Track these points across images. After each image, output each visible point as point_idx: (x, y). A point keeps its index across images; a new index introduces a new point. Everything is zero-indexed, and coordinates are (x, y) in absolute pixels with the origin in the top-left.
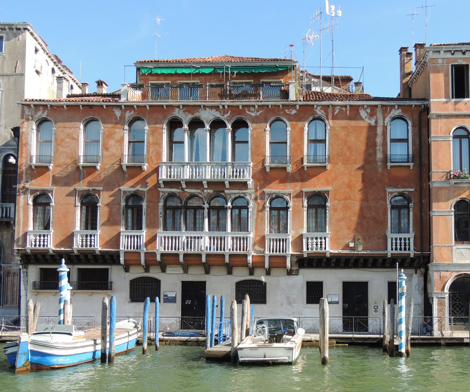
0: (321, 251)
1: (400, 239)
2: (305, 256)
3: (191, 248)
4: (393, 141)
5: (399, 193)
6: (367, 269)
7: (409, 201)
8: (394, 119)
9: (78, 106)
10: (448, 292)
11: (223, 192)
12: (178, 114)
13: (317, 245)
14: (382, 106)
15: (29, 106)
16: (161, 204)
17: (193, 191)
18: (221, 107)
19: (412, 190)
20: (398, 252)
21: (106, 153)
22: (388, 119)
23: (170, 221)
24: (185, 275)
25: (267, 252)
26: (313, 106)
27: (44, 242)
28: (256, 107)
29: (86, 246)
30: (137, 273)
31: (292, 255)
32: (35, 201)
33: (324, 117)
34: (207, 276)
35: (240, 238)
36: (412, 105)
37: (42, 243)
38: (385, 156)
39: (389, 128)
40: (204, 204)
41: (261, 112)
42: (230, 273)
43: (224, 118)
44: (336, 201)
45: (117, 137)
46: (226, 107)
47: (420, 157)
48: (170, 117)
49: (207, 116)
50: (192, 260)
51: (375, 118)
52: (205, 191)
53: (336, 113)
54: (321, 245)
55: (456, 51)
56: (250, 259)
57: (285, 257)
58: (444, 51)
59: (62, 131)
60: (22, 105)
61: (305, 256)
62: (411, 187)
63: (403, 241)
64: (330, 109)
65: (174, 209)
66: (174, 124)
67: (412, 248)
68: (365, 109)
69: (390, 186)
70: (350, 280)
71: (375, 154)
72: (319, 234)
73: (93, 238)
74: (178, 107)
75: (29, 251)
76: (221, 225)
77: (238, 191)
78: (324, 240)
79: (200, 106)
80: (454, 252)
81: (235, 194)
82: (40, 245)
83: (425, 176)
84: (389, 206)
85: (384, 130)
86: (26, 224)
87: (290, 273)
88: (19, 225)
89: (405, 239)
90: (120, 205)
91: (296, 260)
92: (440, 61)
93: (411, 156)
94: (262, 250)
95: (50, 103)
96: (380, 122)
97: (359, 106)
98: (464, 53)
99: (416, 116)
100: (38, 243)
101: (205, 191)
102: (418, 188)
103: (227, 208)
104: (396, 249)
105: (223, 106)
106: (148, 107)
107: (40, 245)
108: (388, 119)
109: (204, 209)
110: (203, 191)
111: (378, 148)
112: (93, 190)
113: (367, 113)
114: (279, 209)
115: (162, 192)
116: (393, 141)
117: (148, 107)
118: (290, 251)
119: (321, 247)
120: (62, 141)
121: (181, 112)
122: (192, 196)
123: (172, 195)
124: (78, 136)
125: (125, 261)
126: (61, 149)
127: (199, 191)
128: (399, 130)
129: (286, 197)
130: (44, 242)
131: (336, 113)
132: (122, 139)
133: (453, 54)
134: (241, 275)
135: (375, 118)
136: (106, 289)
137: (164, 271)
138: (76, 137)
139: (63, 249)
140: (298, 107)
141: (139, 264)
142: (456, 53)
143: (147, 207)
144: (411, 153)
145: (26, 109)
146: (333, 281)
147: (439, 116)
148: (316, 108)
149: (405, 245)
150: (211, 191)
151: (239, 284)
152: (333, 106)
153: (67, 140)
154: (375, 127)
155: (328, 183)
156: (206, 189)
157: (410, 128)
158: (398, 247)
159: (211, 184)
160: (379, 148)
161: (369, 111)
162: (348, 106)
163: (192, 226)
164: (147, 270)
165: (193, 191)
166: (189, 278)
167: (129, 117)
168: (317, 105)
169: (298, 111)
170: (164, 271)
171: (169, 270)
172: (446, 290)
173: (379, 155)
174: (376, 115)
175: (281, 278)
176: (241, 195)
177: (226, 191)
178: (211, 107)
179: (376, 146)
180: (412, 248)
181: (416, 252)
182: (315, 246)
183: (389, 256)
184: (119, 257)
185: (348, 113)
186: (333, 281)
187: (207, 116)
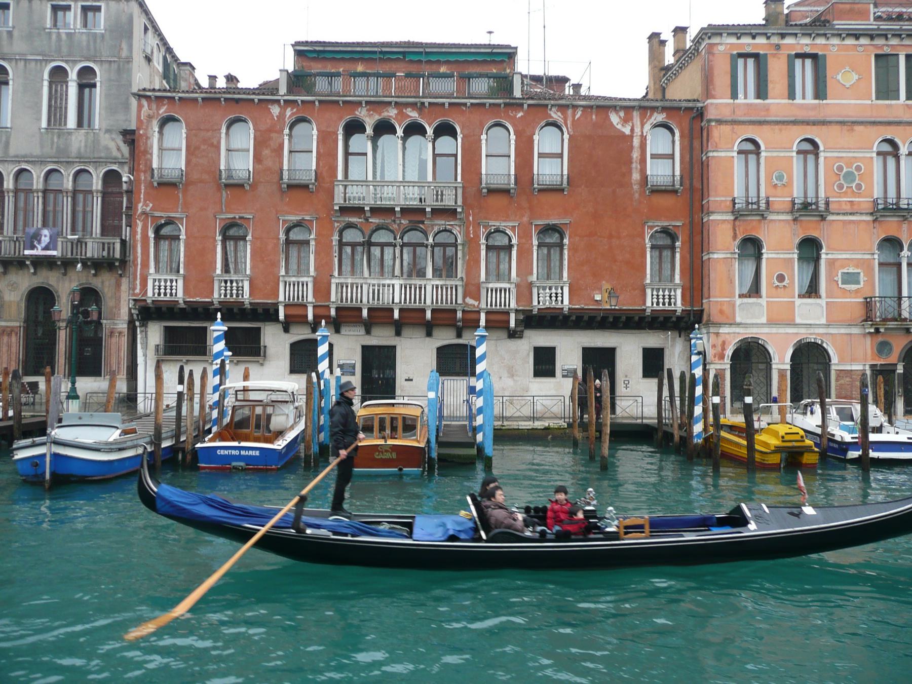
2: (535, 312)
3: (378, 299)
4: (653, 156)
5: (663, 227)
7: (673, 237)
8: (656, 126)
9: (219, 99)
10: (729, 362)
11: (423, 222)
13: (551, 297)
15: (148, 98)
16: (336, 237)
20: (661, 307)
23: (346, 262)
24: (367, 337)
27: (171, 290)
31: (517, 311)
32: (157, 231)
33: (561, 121)
37: (168, 291)
38: (644, 178)
39: (649, 138)
40: (395, 239)
42: (429, 334)
44: (577, 238)
45: (274, 144)
46: (426, 104)
47: (691, 179)
48: (348, 118)
50: (379, 316)
53: (577, 117)
54: (557, 297)
59: (196, 135)
61: (535, 312)
62: (678, 220)
64: (570, 111)
65: (354, 245)
68: (617, 112)
70: (592, 345)
75: (149, 301)
77: (443, 222)
78: (560, 291)
79: (390, 103)
80: (737, 309)
82: (165, 294)
83: (697, 204)
84: (648, 245)
85: (642, 142)
86: (145, 265)
88: (136, 266)
90: (279, 239)
91: (522, 317)
94: (476, 303)
95: (180, 95)
96: (637, 130)
98: (754, 37)
99: (686, 123)
100: (162, 291)
102: (687, 222)
108: (647, 127)
110: (394, 221)
111: (634, 165)
112: (241, 218)
113: (620, 117)
114: (498, 249)
116: (653, 156)
117: (317, 103)
118: (513, 305)
120: (198, 148)
124: (219, 143)
125: (286, 316)
126: (194, 160)
128: (659, 142)
130: (171, 290)
131: (577, 117)
132: (281, 146)
133: (739, 38)
134: (444, 337)
136: (259, 355)
137: (337, 331)
138: (215, 143)
139: (198, 299)
140: (525, 106)
146: (569, 349)
147: (720, 122)
149: (670, 299)
153: (203, 147)
154: (631, 137)
159: (405, 211)
160: (636, 166)
161: (622, 114)
163: (378, 269)
166: (373, 341)
167: (290, 116)
168: (552, 106)
169: (527, 113)
170: (337, 331)
171: (344, 330)
172: (727, 360)
173: (636, 176)
174: (632, 120)
179: (632, 163)
182: (548, 298)
183: (648, 312)
184: (277, 311)
186: (569, 349)
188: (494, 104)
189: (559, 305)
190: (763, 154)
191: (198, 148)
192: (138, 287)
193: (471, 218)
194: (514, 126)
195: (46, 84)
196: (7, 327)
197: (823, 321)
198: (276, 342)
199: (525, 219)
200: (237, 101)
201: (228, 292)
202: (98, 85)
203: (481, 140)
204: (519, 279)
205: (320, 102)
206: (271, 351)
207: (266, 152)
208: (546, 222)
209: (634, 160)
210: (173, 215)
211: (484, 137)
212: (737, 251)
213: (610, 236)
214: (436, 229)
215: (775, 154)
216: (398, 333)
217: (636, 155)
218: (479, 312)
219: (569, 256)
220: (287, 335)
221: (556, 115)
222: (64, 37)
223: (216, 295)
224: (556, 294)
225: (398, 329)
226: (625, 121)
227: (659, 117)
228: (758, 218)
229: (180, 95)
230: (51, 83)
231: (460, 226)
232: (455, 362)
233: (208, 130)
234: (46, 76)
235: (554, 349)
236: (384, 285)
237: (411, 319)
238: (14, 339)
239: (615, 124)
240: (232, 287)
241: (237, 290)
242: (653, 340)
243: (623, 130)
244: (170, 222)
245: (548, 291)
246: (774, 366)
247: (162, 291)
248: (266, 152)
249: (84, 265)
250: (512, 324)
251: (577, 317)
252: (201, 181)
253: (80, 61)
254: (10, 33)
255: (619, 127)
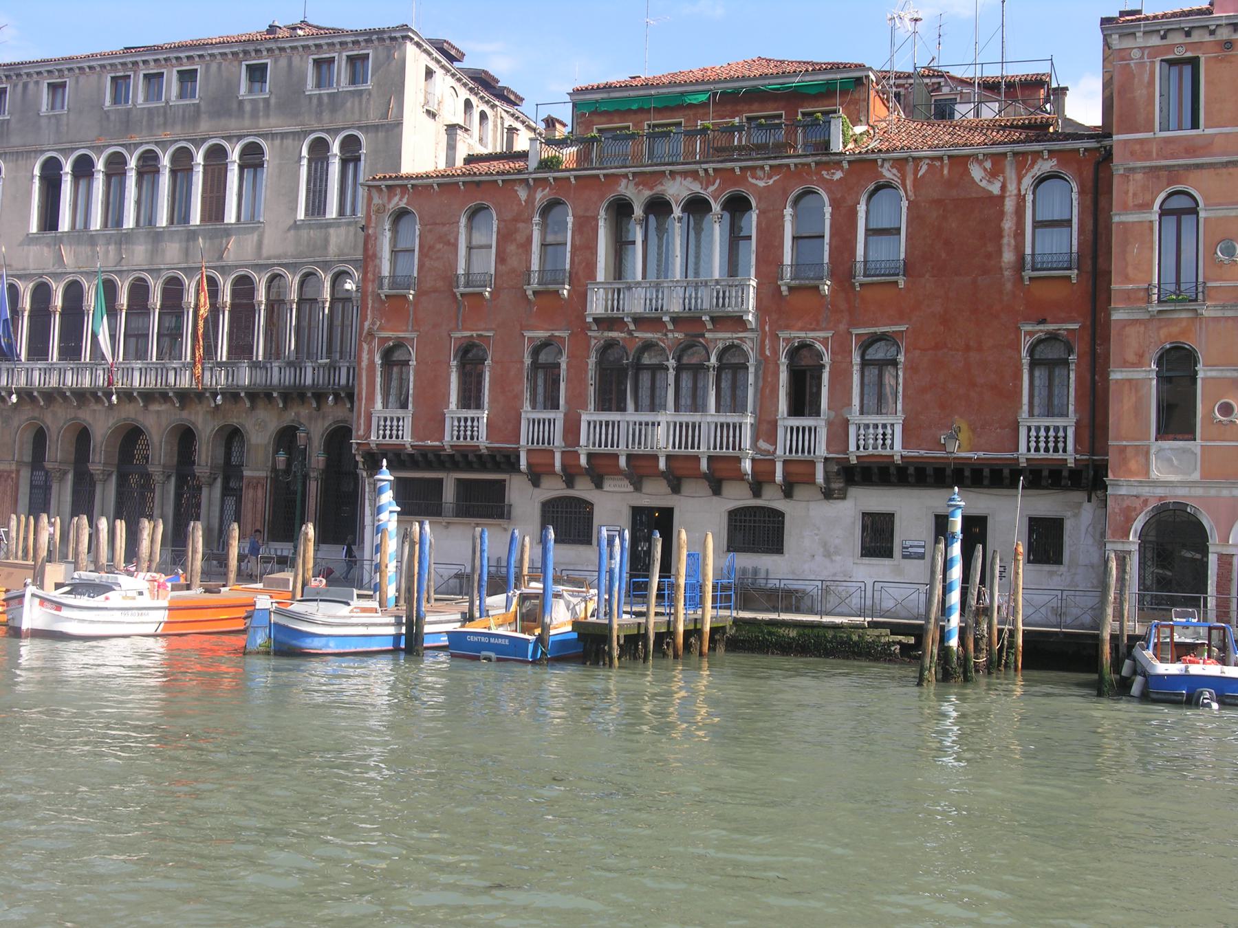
0: (884, 453)
1: (1047, 429)
3: (640, 443)
6: (985, 490)
9: (457, 183)
10: (1136, 540)
11: (703, 336)
12: (626, 189)
14: (1015, 154)
15: (378, 188)
17: (649, 335)
18: (702, 173)
19: (1076, 326)
20: (1042, 454)
21: (503, 268)
22: (1027, 181)
24: (636, 495)
25: (779, 452)
26: (876, 160)
28: (767, 168)
29: (465, 438)
30: (553, 489)
31: (826, 459)
33: (897, 181)
34: (676, 497)
35: (728, 425)
36: (1078, 150)
37: (394, 432)
38: (1021, 257)
39: (1029, 198)
41: (775, 178)
43: (708, 193)
44: (917, 352)
45: (520, 238)
46: (711, 171)
48: (611, 196)
49: (677, 191)
51: (1001, 178)
52: (670, 335)
54: (884, 439)
55: (1169, 30)
56: (747, 466)
57: (812, 463)
58: (1145, 33)
59: (430, 231)
60: (369, 186)
62: (1073, 321)
63: (1052, 433)
64: (910, 167)
66: (621, 209)
67: (1070, 447)
68: (980, 163)
69: (1027, 320)
71: (999, 252)
72: (879, 420)
73: (475, 423)
74: (626, 176)
75: (373, 446)
76: (700, 402)
77: (728, 335)
80: (1153, 458)
81: (724, 339)
82: (391, 437)
84: (1026, 361)
85: (1018, 203)
86: (371, 399)
87: (828, 494)
88: (360, 400)
89: (1057, 429)
90: (522, 362)
91: (835, 468)
92: (1136, 54)
93: (1074, 256)
94: (771, 448)
95: (413, 182)
96: (1012, 188)
97: (968, 156)
98: (1188, 34)
99: (1088, 172)
100: (388, 432)
101: (670, 335)
102: (1088, 323)
103: (708, 368)
104: (1037, 449)
105: (706, 170)
106: (572, 180)
107: (391, 437)
109: (667, 369)
111: (1005, 241)
112: (479, 336)
113: (985, 170)
115: (595, 338)
117: (572, 180)
119: (884, 444)
120: (431, 248)
121: (631, 185)
122: (648, 346)
123: (610, 345)
124: (457, 239)
125: (529, 465)
126: (428, 263)
127: (659, 335)
129: (819, 346)
133: (1164, 37)
134: (738, 497)
135: (1001, 178)
136: (501, 516)
137: (599, 485)
138: (452, 240)
140: (846, 165)
141: (554, 473)
142: (1170, 36)
143: (568, 364)
144: (1075, 249)
145: (375, 195)
148: (882, 166)
150: (679, 335)
151: (734, 515)
152: (914, 159)
153: (439, 246)
154: (1002, 198)
155: (901, 317)
156: (671, 331)
157: (1075, 196)
158: (1042, 445)
160: (1008, 241)
161: (988, 165)
162: (946, 158)
164: (570, 483)
165: (649, 335)
166: (644, 501)
168: (884, 160)
169: (848, 173)
170: (599, 485)
171: (609, 485)
173: (1008, 256)
175: (812, 505)
176: (736, 342)
177: (707, 335)
178: (685, 174)
179: (1001, 237)
180: (1070, 447)
181: (1078, 457)
182: (871, 441)
184: (518, 457)
185: (946, 172)
187: (677, 191)
188: (803, 165)
189: (888, 452)
190: (1202, 214)
191: (431, 248)
192: (362, 427)
193: (767, 328)
194: (829, 192)
195: (305, 162)
196: (253, 478)
197: (1196, 476)
198: (526, 499)
199: (842, 327)
200: (478, 184)
201: (462, 433)
202: (363, 158)
203: (783, 216)
204: (833, 414)
205: (576, 177)
206: (516, 512)
207: (511, 248)
208: (872, 330)
209: (1006, 233)
210: (402, 335)
211: (788, 211)
212: (1154, 367)
213: (968, 348)
214: (720, 345)
215: (1221, 213)
216: (676, 489)
217: (1008, 225)
218: (773, 462)
219: (904, 379)
220: (537, 491)
221: (888, 173)
222: (326, 100)
223: (447, 438)
224: (884, 434)
225: (675, 483)
226: (992, 175)
227: (1046, 166)
228: (1190, 315)
229: (413, 182)
230: (309, 160)
231: (752, 340)
232: (756, 531)
233: (444, 224)
234: (305, 152)
235: (891, 516)
236: (647, 424)
237: (678, 473)
238: (260, 493)
239: (977, 179)
240: (466, 427)
241: (472, 431)
242: (1046, 504)
243: (990, 188)
244: (400, 344)
245: (871, 430)
246: (1211, 549)
247: (388, 432)
248: (511, 248)
249: (337, 397)
250: (820, 477)
251: (916, 469)
252: (435, 290)
253: (343, 129)
254: (266, 101)
255: (984, 184)
